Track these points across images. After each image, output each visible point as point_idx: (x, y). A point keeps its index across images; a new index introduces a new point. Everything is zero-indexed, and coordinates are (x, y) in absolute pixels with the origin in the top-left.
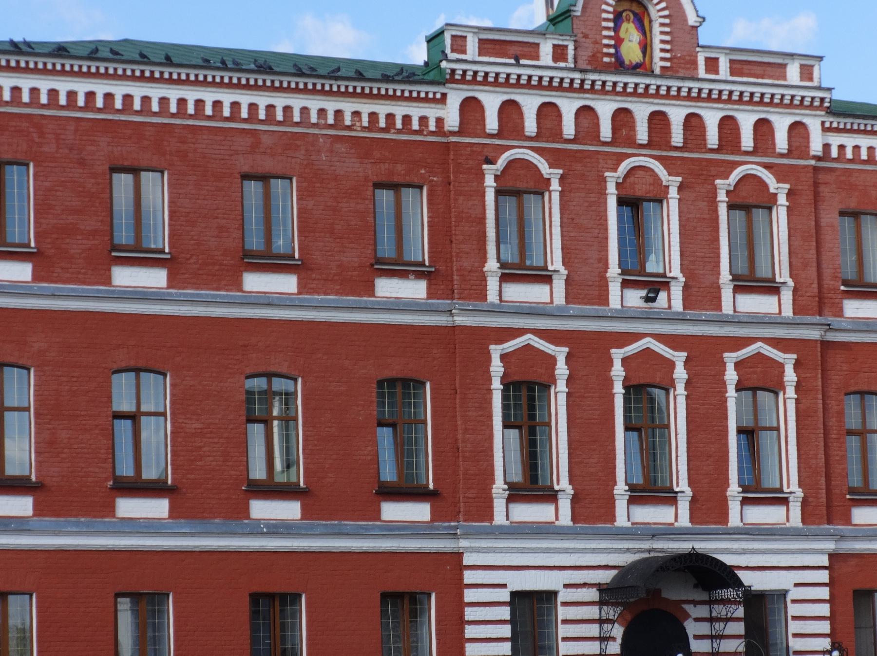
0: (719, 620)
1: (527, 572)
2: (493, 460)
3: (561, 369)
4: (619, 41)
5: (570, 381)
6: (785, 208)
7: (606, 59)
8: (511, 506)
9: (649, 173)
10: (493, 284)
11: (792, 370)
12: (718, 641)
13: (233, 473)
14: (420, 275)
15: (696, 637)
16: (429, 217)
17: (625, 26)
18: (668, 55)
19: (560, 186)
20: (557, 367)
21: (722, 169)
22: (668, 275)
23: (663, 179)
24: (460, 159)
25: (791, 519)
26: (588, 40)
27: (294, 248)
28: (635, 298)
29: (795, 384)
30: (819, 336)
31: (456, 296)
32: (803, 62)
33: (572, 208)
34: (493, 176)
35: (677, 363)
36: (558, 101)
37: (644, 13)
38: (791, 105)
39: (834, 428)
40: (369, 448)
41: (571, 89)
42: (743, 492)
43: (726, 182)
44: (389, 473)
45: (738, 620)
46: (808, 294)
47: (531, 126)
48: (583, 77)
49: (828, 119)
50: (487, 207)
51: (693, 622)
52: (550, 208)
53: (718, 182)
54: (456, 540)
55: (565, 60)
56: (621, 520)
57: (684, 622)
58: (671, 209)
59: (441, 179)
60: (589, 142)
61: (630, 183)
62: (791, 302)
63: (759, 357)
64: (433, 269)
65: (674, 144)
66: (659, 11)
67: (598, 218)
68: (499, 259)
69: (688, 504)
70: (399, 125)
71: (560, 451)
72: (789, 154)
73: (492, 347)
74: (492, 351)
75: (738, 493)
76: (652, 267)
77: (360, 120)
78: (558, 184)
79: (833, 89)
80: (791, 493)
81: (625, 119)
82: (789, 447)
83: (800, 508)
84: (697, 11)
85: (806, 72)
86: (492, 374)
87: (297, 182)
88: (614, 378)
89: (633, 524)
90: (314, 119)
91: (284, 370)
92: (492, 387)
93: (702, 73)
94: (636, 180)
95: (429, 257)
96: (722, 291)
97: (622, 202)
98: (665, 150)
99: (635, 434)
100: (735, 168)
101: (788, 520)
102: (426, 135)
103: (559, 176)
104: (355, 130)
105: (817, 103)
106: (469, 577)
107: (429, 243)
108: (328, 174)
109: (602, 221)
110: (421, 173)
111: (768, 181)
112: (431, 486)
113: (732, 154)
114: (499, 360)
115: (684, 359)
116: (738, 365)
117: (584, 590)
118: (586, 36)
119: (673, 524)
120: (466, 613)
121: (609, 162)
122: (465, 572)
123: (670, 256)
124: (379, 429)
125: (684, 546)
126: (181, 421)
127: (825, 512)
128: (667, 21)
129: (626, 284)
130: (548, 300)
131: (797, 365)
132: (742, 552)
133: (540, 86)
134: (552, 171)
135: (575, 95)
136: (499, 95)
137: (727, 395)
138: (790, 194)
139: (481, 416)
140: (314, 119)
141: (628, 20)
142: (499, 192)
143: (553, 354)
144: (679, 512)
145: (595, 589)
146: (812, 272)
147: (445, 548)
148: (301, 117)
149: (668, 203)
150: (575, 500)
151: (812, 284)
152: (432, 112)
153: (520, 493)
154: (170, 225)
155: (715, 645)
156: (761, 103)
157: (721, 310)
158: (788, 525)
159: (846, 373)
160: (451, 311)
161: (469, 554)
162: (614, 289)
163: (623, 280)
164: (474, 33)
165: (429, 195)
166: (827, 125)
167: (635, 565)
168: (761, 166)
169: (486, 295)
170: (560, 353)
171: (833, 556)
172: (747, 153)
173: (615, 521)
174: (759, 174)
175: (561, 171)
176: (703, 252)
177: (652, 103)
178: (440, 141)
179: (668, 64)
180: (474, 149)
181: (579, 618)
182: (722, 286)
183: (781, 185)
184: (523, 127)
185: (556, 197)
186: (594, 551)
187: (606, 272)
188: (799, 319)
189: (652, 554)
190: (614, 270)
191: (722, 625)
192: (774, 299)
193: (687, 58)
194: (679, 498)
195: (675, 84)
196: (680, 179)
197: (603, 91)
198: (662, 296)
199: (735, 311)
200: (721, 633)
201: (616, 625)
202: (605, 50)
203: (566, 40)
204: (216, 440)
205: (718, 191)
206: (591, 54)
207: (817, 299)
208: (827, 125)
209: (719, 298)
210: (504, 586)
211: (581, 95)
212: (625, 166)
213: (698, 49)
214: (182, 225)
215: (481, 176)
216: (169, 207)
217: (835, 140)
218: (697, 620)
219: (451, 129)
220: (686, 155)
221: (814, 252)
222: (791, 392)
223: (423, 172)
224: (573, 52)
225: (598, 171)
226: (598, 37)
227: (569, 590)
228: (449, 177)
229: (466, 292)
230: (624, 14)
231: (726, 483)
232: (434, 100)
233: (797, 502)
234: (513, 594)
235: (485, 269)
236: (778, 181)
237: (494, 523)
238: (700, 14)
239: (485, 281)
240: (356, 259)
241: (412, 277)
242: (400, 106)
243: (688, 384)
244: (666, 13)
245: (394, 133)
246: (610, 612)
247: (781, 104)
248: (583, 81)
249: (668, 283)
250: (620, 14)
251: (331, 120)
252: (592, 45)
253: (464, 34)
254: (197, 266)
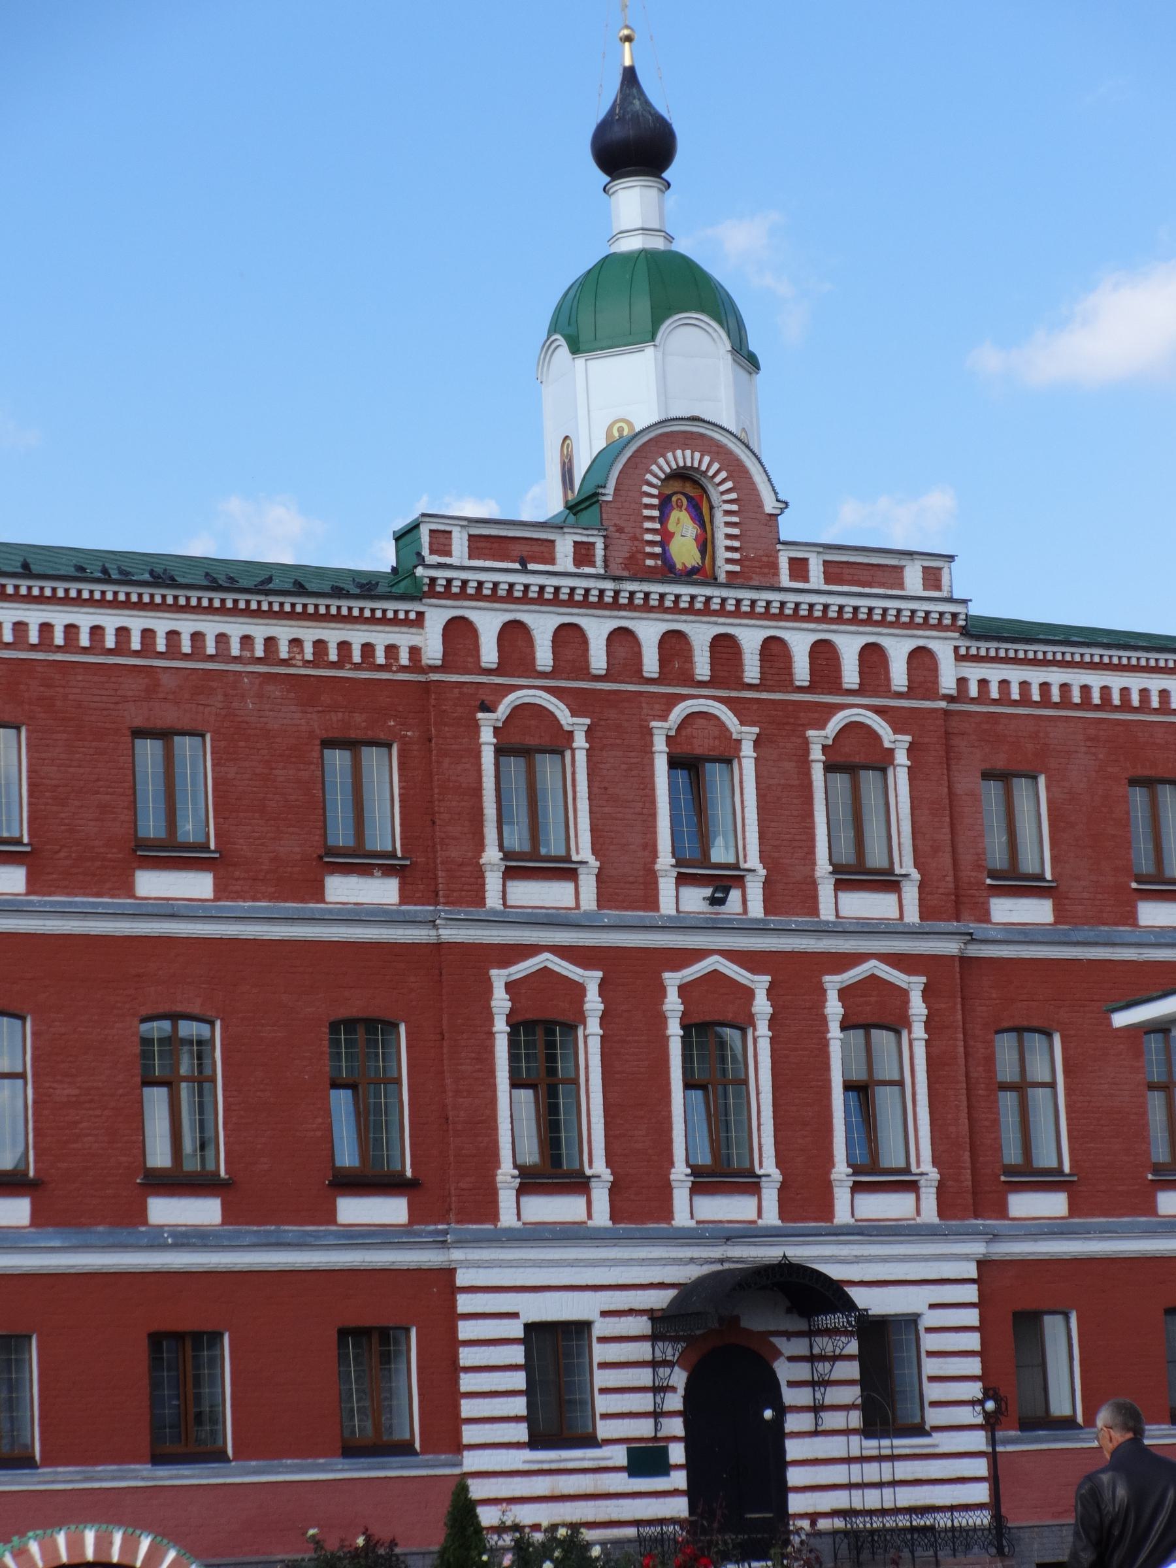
0: (823, 1358)
1: (548, 1295)
2: (497, 1135)
3: (593, 1002)
4: (667, 537)
5: (604, 1020)
6: (906, 769)
7: (650, 562)
8: (525, 1200)
9: (712, 722)
10: (493, 882)
11: (920, 999)
12: (822, 1389)
13: (123, 1159)
14: (389, 871)
15: (792, 1384)
16: (400, 788)
17: (675, 515)
18: (737, 556)
19: (586, 742)
20: (587, 999)
21: (816, 715)
22: (743, 865)
23: (733, 730)
24: (446, 705)
25: (923, 1212)
26: (623, 536)
27: (208, 834)
28: (695, 899)
29: (924, 1018)
30: (957, 950)
31: (442, 900)
32: (926, 564)
33: (605, 772)
34: (492, 729)
35: (757, 991)
36: (583, 622)
37: (702, 497)
38: (911, 625)
39: (981, 1080)
40: (320, 1120)
41: (600, 604)
42: (854, 1174)
43: (822, 733)
44: (347, 1155)
45: (849, 1358)
46: (941, 891)
47: (544, 657)
48: (617, 588)
49: (963, 643)
50: (484, 773)
51: (786, 1362)
52: (574, 773)
53: (811, 733)
54: (446, 1250)
55: (592, 564)
56: (681, 1218)
57: (773, 1363)
58: (745, 772)
59: (417, 734)
60: (627, 679)
61: (686, 736)
62: (917, 902)
63: (873, 980)
64: (408, 863)
65: (747, 680)
66: (723, 493)
67: (642, 786)
68: (501, 847)
69: (776, 1192)
70: (357, 657)
71: (593, 1120)
72: (910, 694)
73: (494, 972)
74: (493, 979)
75: (848, 1176)
76: (720, 854)
77: (302, 651)
78: (584, 739)
79: (970, 600)
80: (922, 1174)
81: (678, 647)
82: (918, 1109)
83: (935, 1196)
84: (776, 493)
85: (932, 578)
86: (495, 1010)
87: (212, 740)
88: (668, 1014)
89: (698, 1222)
90: (235, 651)
91: (196, 1009)
92: (495, 1029)
93: (785, 580)
94: (695, 733)
95: (402, 845)
96: (820, 887)
97: (674, 763)
98: (735, 690)
99: (699, 1093)
100: (834, 714)
101: (918, 1213)
102: (395, 672)
103: (585, 728)
104: (294, 666)
105: (947, 621)
106: (464, 1303)
107: (402, 825)
108: (256, 728)
109: (647, 791)
110: (390, 726)
111: (881, 731)
112: (409, 1173)
113: (830, 693)
114: (503, 990)
115: (767, 985)
116: (844, 994)
117: (630, 1319)
118: (620, 530)
119: (754, 1222)
120: (461, 1356)
121: (657, 706)
122: (458, 1297)
123: (744, 839)
124: (333, 1092)
125: (771, 1253)
126: (47, 1085)
127: (971, 1201)
128: (735, 507)
129: (683, 880)
130: (572, 904)
131: (927, 993)
132: (855, 1259)
133: (556, 601)
134: (576, 720)
135: (607, 613)
136: (499, 613)
137: (830, 1035)
138: (911, 750)
139: (480, 1071)
140: (235, 651)
141: (680, 507)
142: (500, 751)
143: (581, 981)
144: (764, 1204)
145: (645, 1318)
146: (946, 859)
147: (430, 1261)
148: (216, 648)
149: (740, 764)
150: (615, 1190)
152: (404, 639)
153: (537, 1181)
154: (30, 804)
155: (818, 1396)
156: (869, 621)
157: (818, 915)
158: (919, 1220)
159: (997, 1001)
160: (434, 921)
161: (464, 1270)
162: (666, 887)
163: (679, 873)
164: (462, 526)
165: (400, 756)
166: (963, 651)
167: (701, 1281)
169: (484, 898)
170: (591, 979)
171: (982, 1264)
172: (850, 692)
173: (673, 1219)
174: (868, 722)
175: (588, 721)
176: (790, 833)
177: (716, 623)
178: (416, 679)
179: (737, 568)
180: (465, 690)
181: (623, 1359)
182: (819, 881)
183: (899, 737)
184: (534, 659)
185: (581, 757)
186: (643, 1262)
187: (654, 862)
188: (929, 925)
189: (727, 1266)
190: (665, 860)
191: (827, 1365)
192: (892, 898)
193: (765, 559)
194: (763, 1185)
195: (746, 595)
196: (756, 730)
197: (646, 607)
198: (735, 895)
199: (837, 916)
200: (826, 1378)
201: (676, 1369)
202: (648, 549)
203: (593, 535)
204: (98, 1112)
205: (812, 746)
206: (627, 555)
207: (953, 897)
208: (963, 651)
209: (814, 898)
210: (515, 1315)
211: (616, 613)
212: (678, 713)
213: (779, 547)
214: (47, 804)
215: (476, 727)
216: (29, 778)
217: (973, 673)
218: (792, 1359)
219: (431, 662)
220: (765, 695)
221: (947, 830)
222: (919, 1031)
223: (392, 723)
224: (602, 553)
225: (641, 720)
226: (638, 531)
227: (608, 1320)
228: (429, 730)
229: (455, 894)
230: (674, 499)
231: (829, 1162)
232: (406, 622)
233: (931, 1187)
234: (528, 1327)
235: (482, 861)
236: (896, 731)
237: (499, 1225)
238: (781, 497)
239: (483, 878)
240: (297, 850)
241: (377, 873)
242: (358, 630)
243: (773, 1022)
244: (733, 496)
245: (350, 669)
246: (669, 1351)
247: (896, 624)
248: (617, 593)
249: (743, 877)
250: (669, 497)
251: (259, 652)
252: (629, 542)
253: (448, 528)
254: (69, 862)
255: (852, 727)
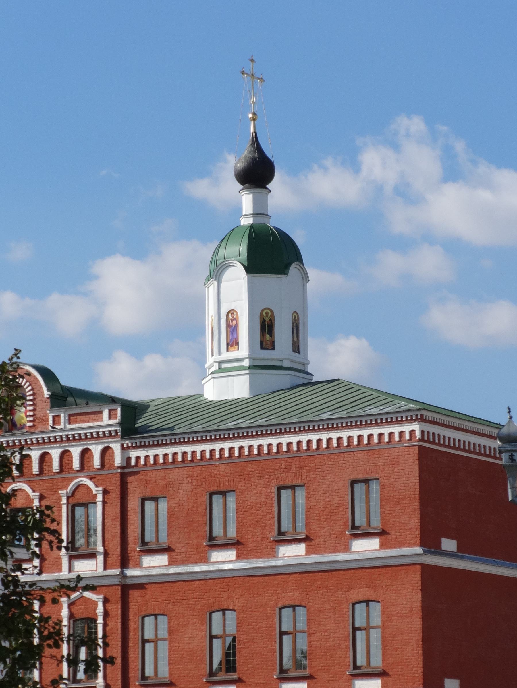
21: (65, 483)
30: (118, 582)
46: (114, 556)
53: (61, 492)
151: (117, 548)
159: (140, 603)
166: (125, 446)
168: (87, 478)
217: (133, 454)
255: (79, 486)
